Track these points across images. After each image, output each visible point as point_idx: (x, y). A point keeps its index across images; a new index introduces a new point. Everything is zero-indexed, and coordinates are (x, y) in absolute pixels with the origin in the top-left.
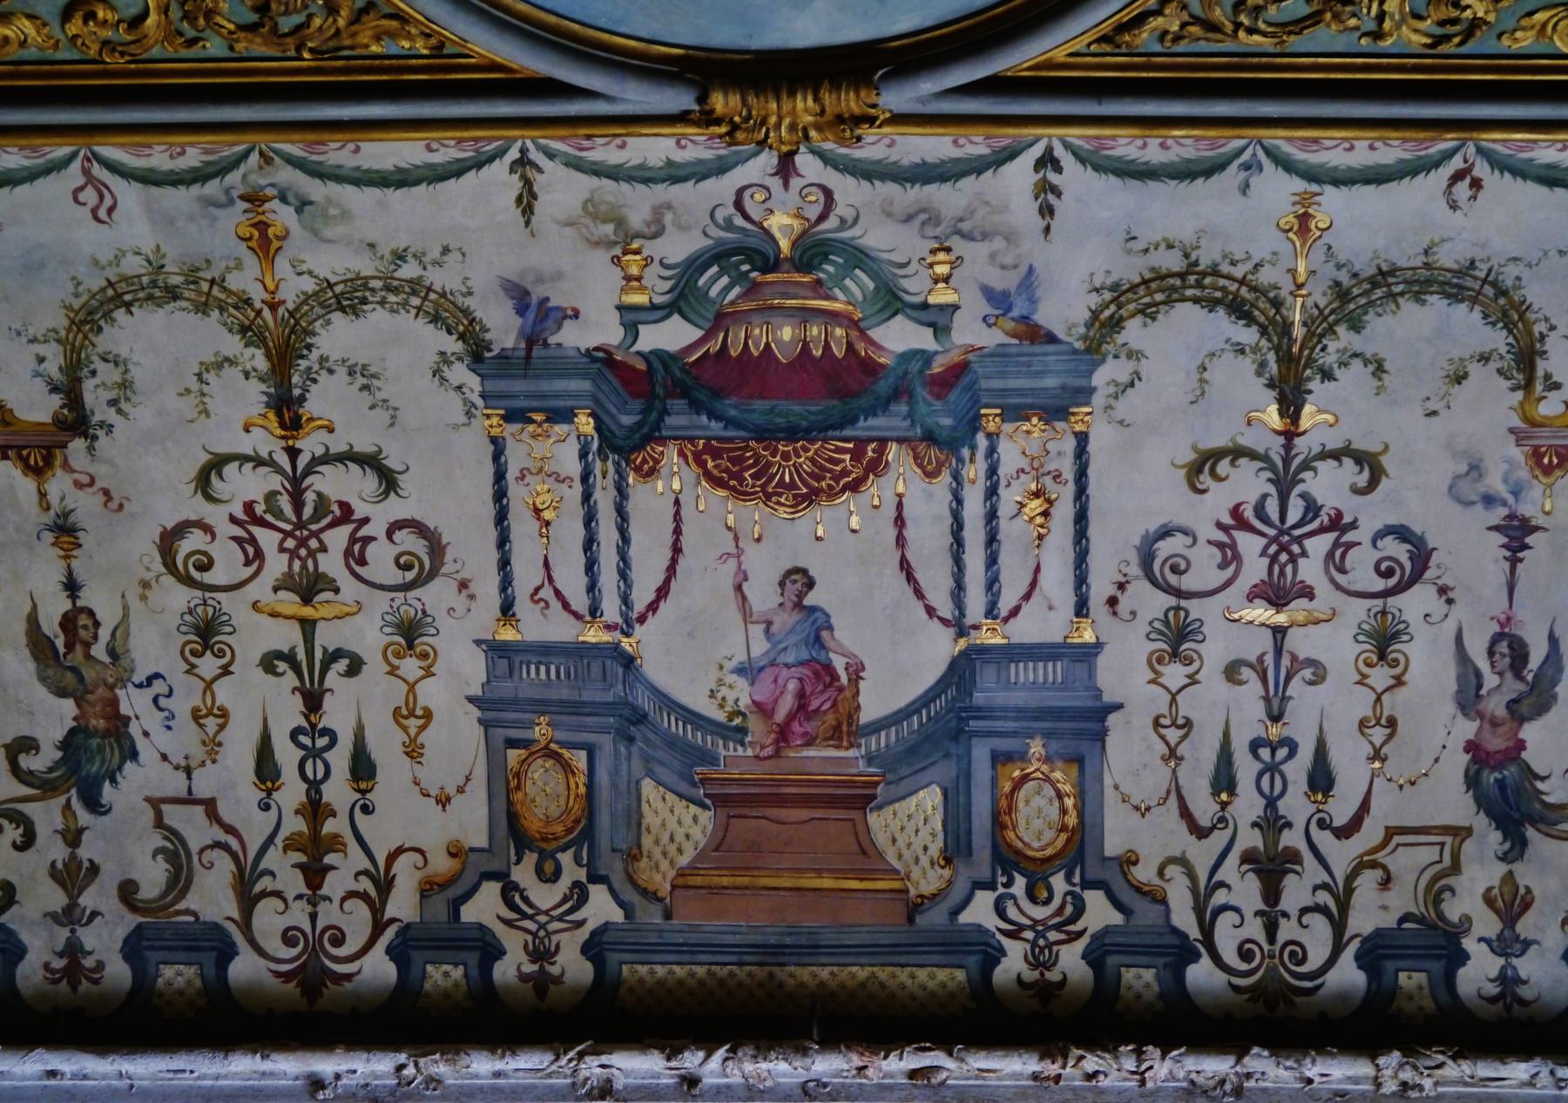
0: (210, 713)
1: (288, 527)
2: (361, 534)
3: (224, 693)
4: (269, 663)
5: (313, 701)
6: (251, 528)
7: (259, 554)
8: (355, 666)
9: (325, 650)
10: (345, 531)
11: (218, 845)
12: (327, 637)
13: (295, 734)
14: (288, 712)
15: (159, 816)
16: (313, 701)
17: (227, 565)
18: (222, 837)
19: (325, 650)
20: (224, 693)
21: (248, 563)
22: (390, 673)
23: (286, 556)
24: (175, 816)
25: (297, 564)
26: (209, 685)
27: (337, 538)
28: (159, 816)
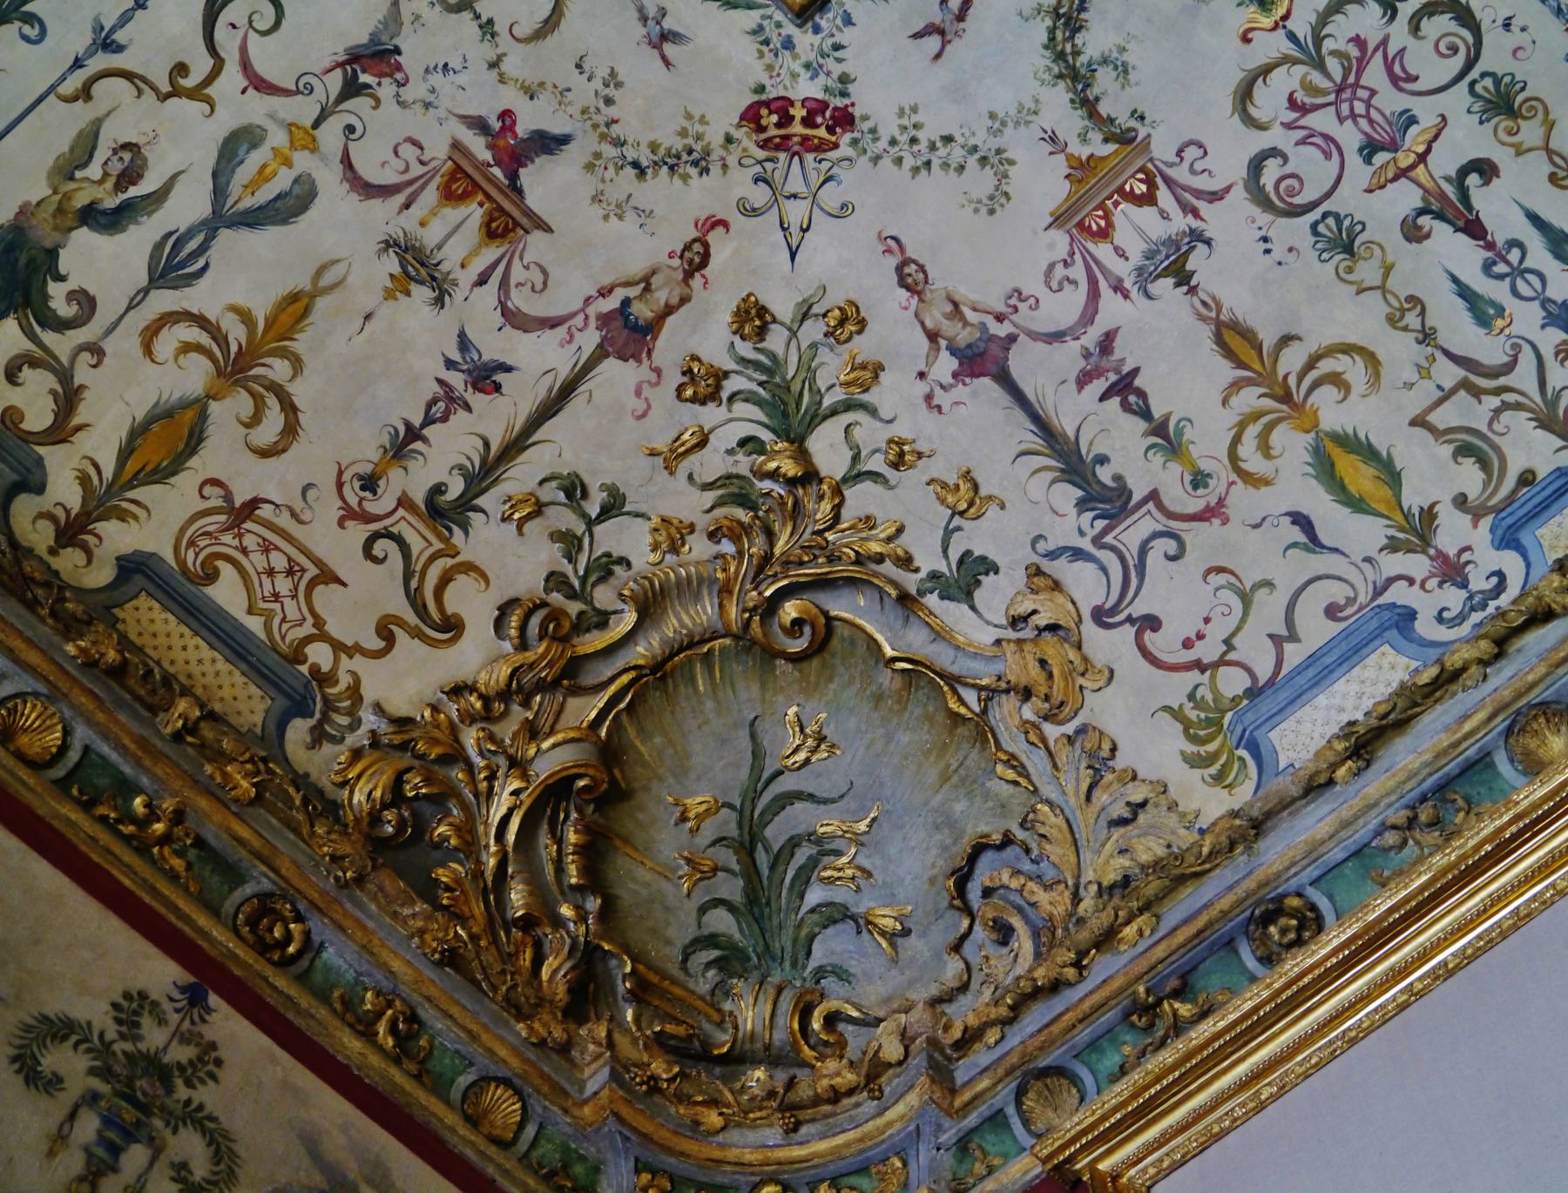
0: (1403, 311)
1: (1332, 98)
2: (1391, 54)
3: (1401, 285)
4: (1413, 232)
5: (1474, 229)
6: (1302, 122)
7: (1327, 138)
8: (1485, 169)
9: (1448, 179)
10: (1377, 62)
11: (1497, 412)
12: (1444, 163)
13: (1487, 267)
14: (1463, 255)
15: (1431, 428)
16: (1474, 229)
17: (1314, 169)
18: (1495, 402)
19: (1448, 179)
20: (1401, 285)
21: (1328, 156)
22: (1519, 153)
23: (1349, 122)
24: (1440, 418)
25: (1363, 123)
26: (1382, 288)
27: (1375, 74)
28: (1431, 428)
